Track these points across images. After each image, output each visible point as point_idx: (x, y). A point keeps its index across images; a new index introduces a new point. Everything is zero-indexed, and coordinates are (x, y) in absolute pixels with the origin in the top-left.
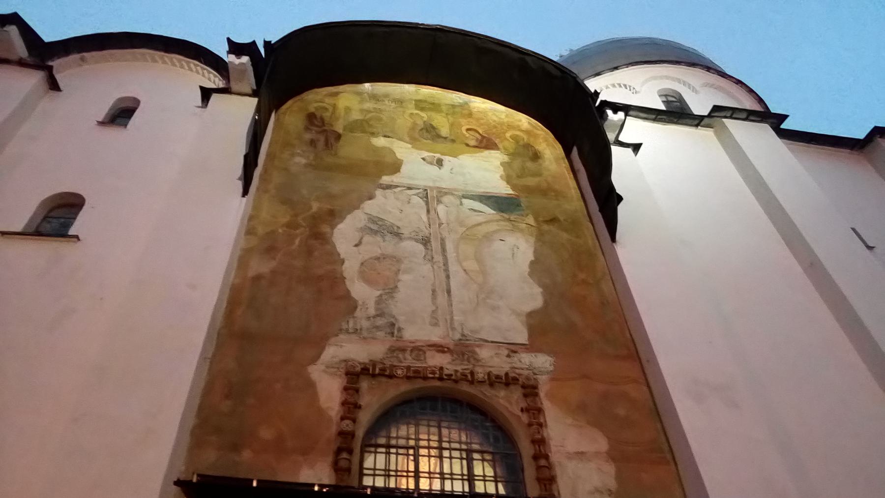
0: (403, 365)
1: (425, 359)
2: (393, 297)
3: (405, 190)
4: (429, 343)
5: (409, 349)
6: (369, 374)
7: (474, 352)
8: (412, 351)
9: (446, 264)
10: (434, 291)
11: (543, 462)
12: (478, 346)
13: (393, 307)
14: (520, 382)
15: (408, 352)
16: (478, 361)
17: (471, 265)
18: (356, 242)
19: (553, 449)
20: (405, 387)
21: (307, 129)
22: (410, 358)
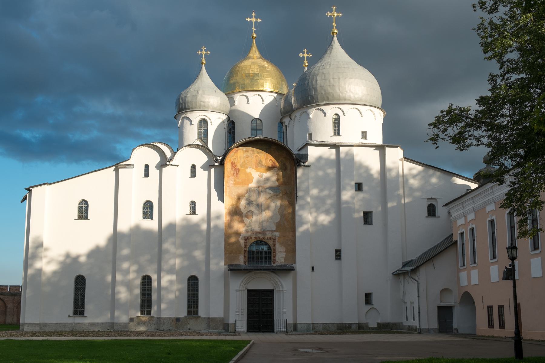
7: (266, 233)
12: (267, 232)
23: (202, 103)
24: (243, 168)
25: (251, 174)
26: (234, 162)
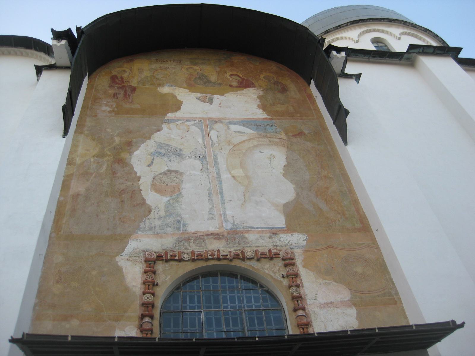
0: (188, 251)
1: (205, 245)
2: (178, 202)
3: (184, 122)
4: (209, 233)
5: (193, 239)
6: (162, 260)
7: (244, 237)
8: (195, 240)
9: (218, 173)
11: (300, 312)
12: (247, 232)
13: (179, 208)
14: (281, 255)
15: (192, 241)
16: (249, 243)
17: (238, 172)
19: (308, 302)
20: (190, 267)
21: (111, 86)
22: (193, 245)
24: (147, 86)
25: (174, 96)
26: (119, 76)
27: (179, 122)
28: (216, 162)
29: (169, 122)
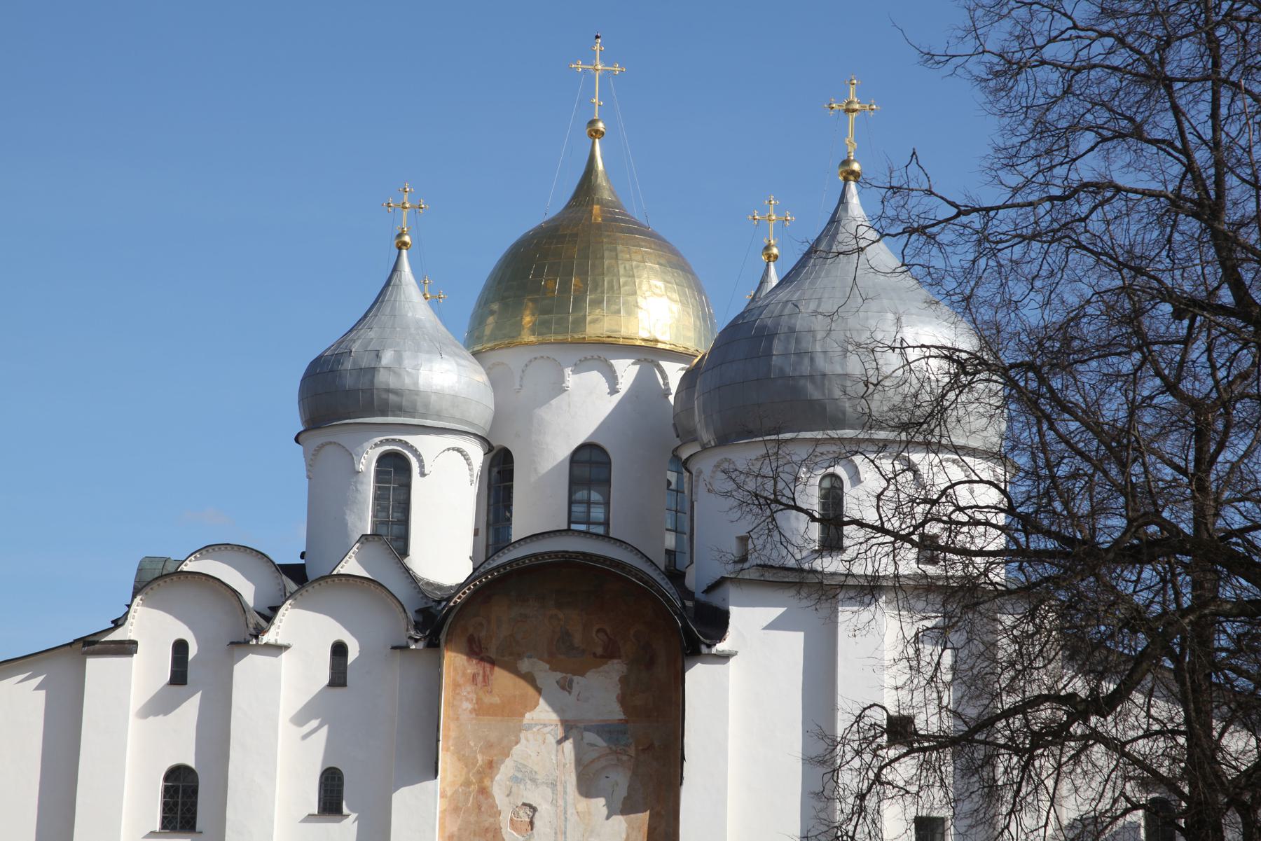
10: (556, 833)
18: (507, 792)
23: (392, 397)
24: (506, 659)
27: (538, 727)
28: (565, 792)
29: (529, 728)
